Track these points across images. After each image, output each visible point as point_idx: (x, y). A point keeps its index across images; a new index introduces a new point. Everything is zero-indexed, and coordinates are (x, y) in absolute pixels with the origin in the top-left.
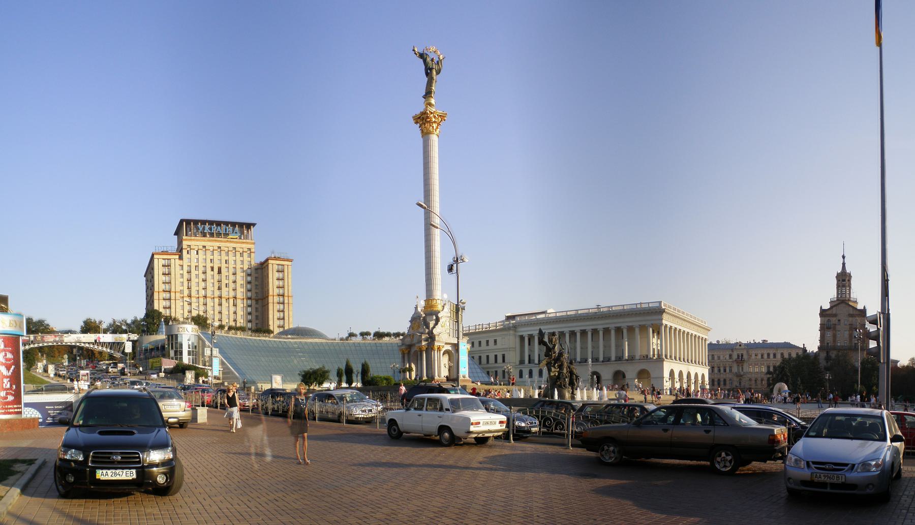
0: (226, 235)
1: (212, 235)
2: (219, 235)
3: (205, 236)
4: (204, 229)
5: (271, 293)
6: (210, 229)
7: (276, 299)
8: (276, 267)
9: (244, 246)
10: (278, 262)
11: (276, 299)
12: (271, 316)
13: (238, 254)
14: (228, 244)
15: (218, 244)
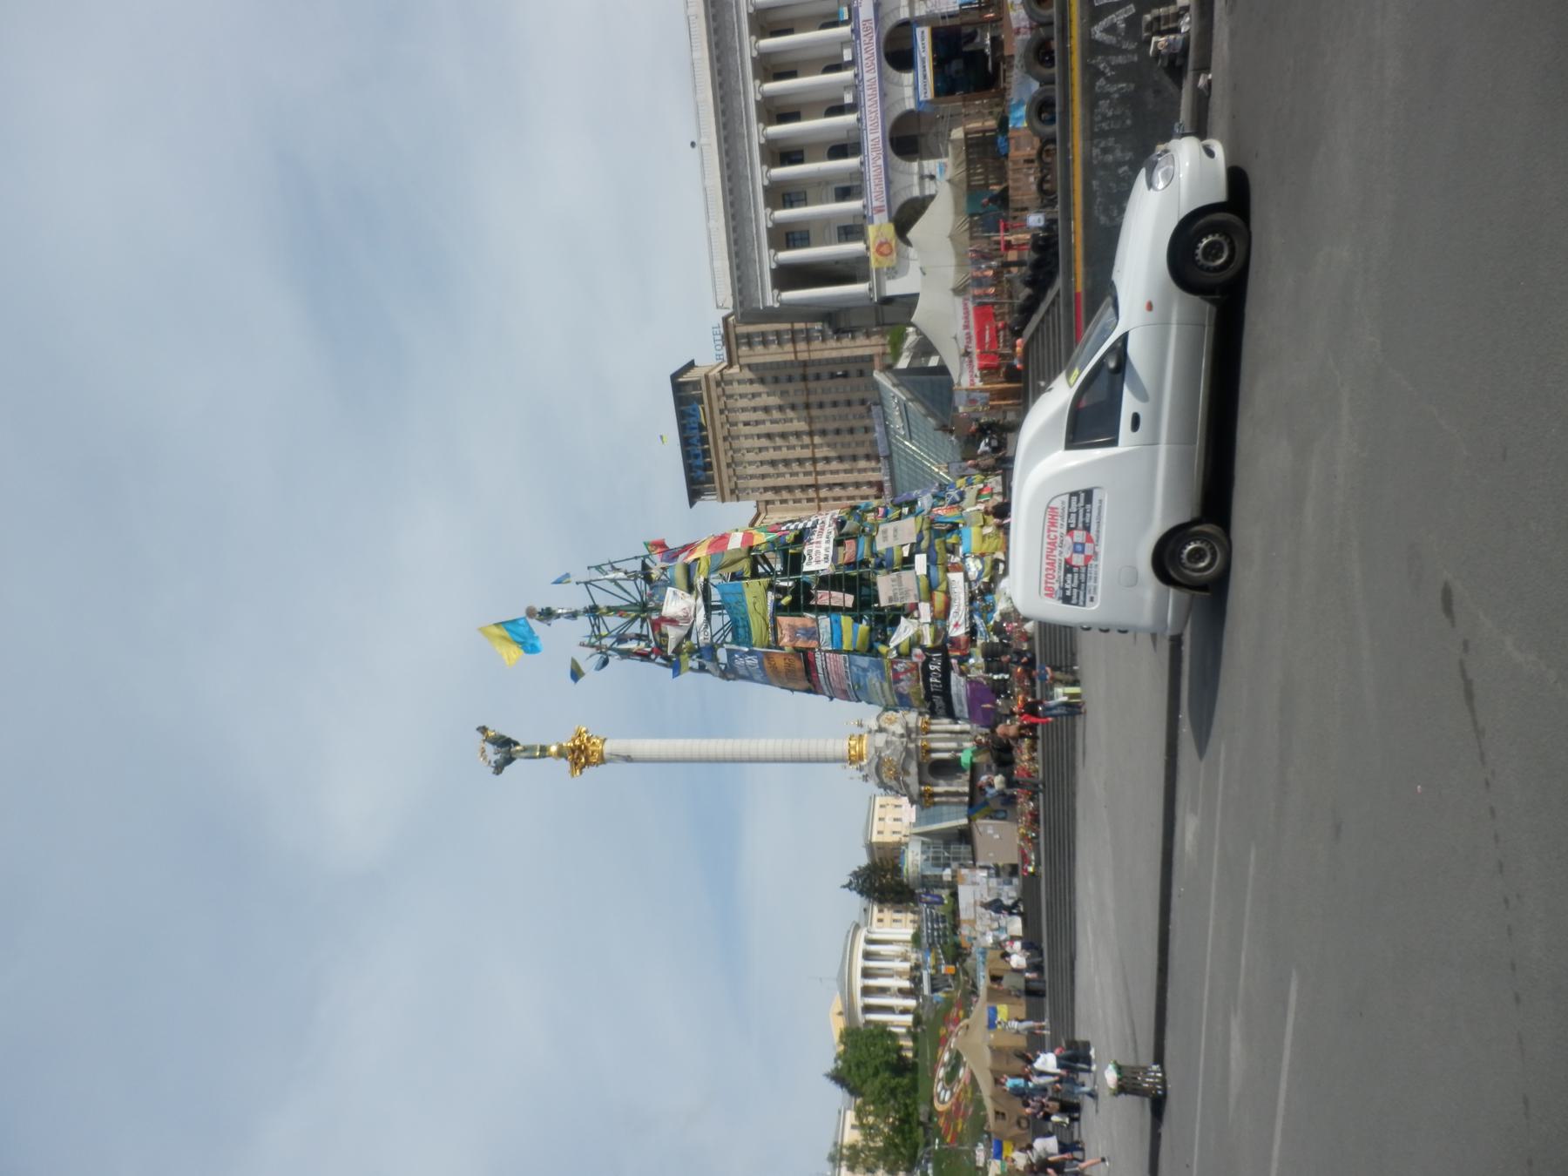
0: (702, 428)
1: (706, 453)
2: (704, 440)
3: (708, 467)
4: (698, 467)
5: (792, 357)
6: (697, 456)
7: (802, 346)
8: (744, 349)
9: (714, 395)
10: (734, 347)
11: (802, 346)
12: (834, 354)
13: (730, 402)
14: (718, 424)
15: (720, 442)
